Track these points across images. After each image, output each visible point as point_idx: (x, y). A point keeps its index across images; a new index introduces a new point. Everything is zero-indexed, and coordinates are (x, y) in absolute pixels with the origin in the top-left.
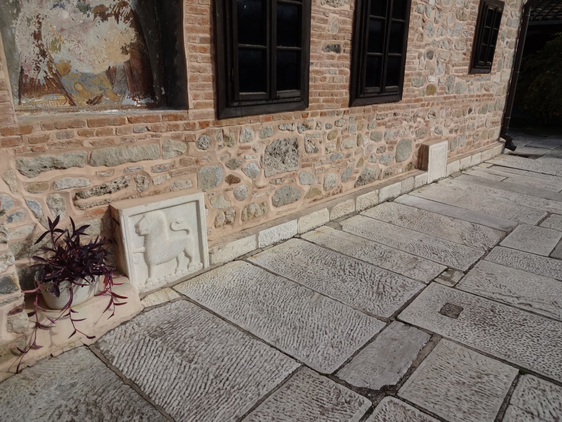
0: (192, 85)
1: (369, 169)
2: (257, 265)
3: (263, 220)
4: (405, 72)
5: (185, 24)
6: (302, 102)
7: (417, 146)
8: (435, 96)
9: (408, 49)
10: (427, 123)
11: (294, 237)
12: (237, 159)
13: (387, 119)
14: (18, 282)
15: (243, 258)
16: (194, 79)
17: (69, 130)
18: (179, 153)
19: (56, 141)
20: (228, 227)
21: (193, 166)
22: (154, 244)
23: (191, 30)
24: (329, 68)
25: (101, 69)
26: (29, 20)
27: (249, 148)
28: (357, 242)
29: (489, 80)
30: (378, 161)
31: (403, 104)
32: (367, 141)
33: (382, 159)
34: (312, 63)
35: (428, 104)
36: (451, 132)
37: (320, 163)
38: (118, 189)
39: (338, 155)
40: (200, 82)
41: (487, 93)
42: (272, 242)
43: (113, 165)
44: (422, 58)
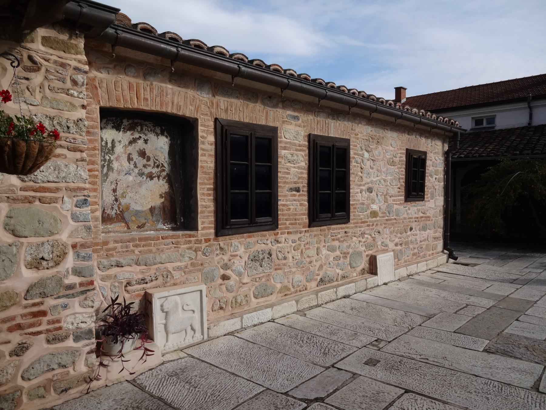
0: (201, 216)
1: (328, 272)
2: (241, 338)
3: (246, 308)
4: (351, 202)
6: (274, 225)
7: (367, 256)
8: (378, 219)
9: (351, 187)
10: (374, 239)
11: (269, 321)
12: (229, 263)
13: (339, 236)
14: (94, 333)
15: (231, 334)
16: (203, 212)
17: (128, 243)
18: (191, 259)
19: (120, 250)
20: (221, 312)
21: (199, 267)
22: (171, 319)
23: (202, 184)
24: (292, 202)
25: (147, 207)
26: (111, 182)
27: (237, 255)
29: (425, 205)
30: (335, 267)
31: (352, 225)
32: (324, 251)
33: (338, 265)
34: (280, 200)
35: (373, 225)
36: (396, 245)
37: (288, 268)
38: (152, 281)
39: (302, 262)
41: (424, 215)
42: (253, 323)
43: (150, 265)
44: (364, 192)
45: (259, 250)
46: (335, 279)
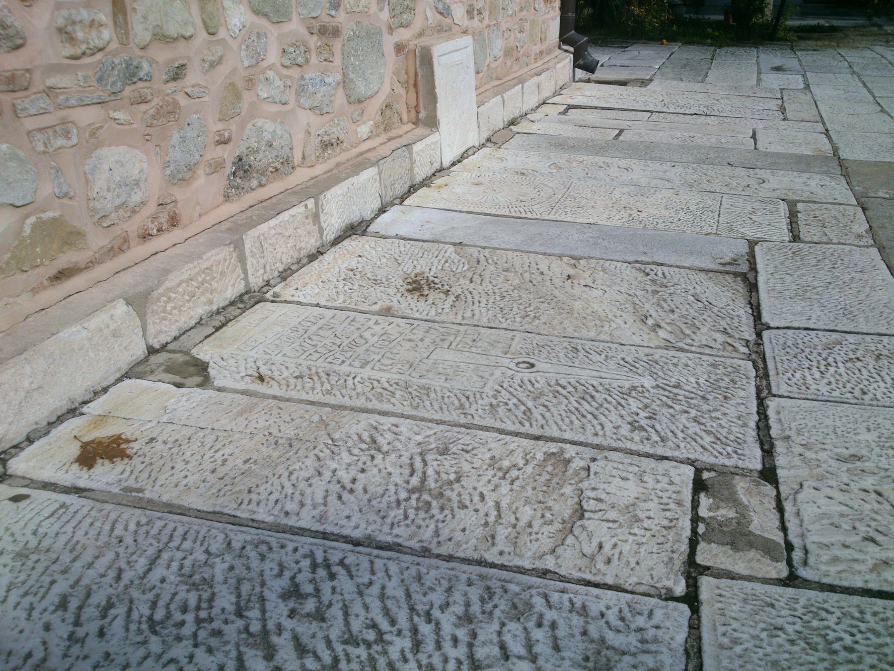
28: (289, 431)
30: (291, 96)
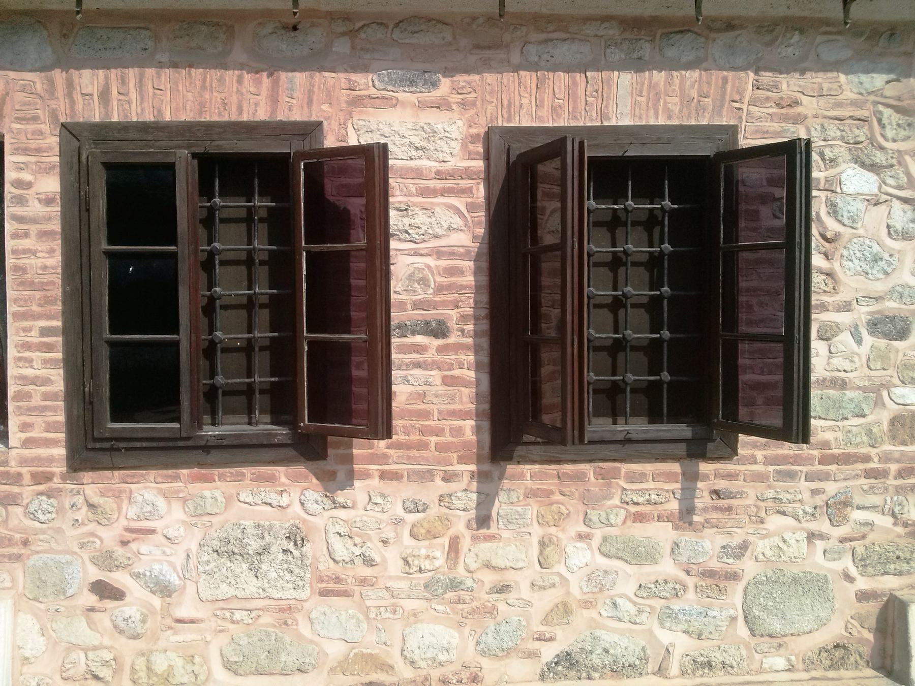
5: (11, 308)
12: (120, 551)
27: (152, 531)
40: (37, 401)
45: (248, 523)
46: (651, 667)
